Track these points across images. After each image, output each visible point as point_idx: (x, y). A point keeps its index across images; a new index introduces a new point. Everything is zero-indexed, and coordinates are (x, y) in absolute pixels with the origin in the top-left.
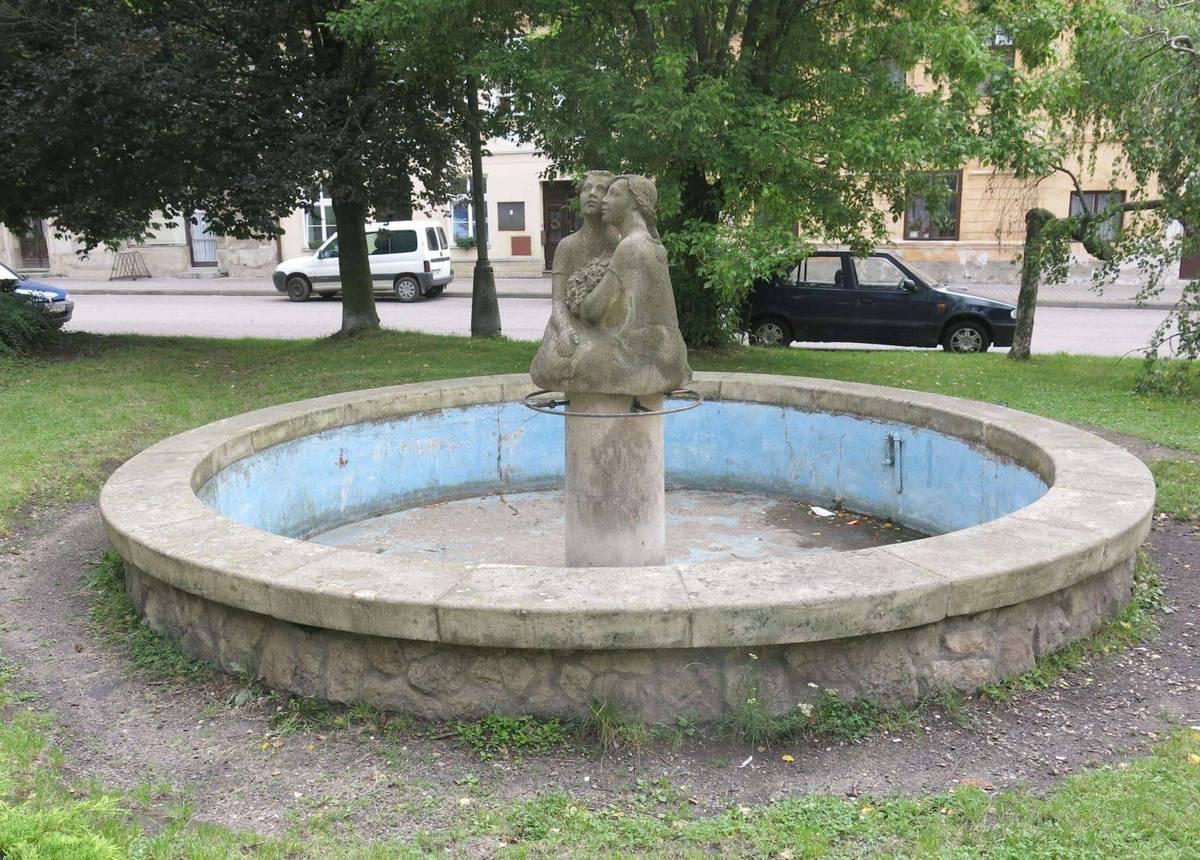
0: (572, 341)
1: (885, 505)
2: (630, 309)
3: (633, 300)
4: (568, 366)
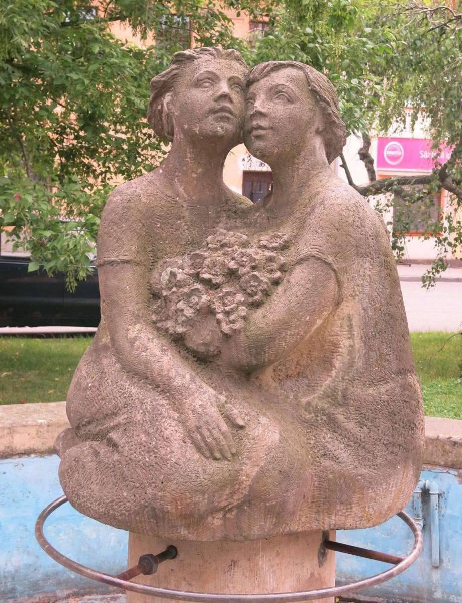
0: (230, 420)
1: (409, 587)
2: (345, 343)
3: (356, 322)
4: (233, 481)
